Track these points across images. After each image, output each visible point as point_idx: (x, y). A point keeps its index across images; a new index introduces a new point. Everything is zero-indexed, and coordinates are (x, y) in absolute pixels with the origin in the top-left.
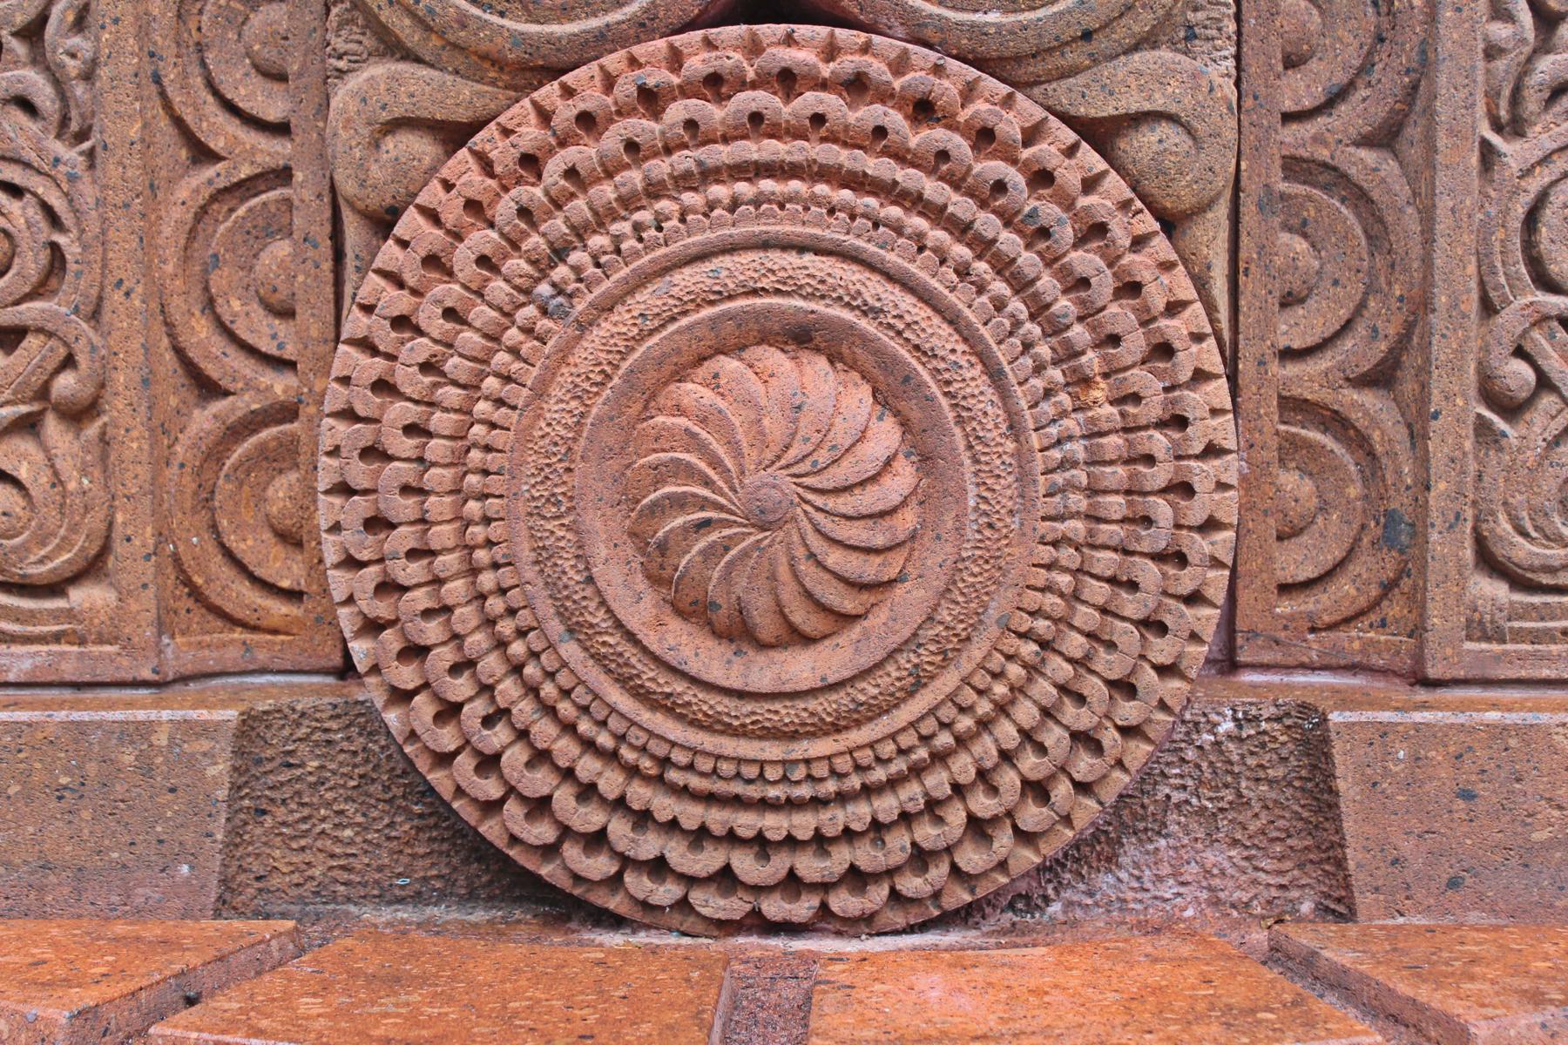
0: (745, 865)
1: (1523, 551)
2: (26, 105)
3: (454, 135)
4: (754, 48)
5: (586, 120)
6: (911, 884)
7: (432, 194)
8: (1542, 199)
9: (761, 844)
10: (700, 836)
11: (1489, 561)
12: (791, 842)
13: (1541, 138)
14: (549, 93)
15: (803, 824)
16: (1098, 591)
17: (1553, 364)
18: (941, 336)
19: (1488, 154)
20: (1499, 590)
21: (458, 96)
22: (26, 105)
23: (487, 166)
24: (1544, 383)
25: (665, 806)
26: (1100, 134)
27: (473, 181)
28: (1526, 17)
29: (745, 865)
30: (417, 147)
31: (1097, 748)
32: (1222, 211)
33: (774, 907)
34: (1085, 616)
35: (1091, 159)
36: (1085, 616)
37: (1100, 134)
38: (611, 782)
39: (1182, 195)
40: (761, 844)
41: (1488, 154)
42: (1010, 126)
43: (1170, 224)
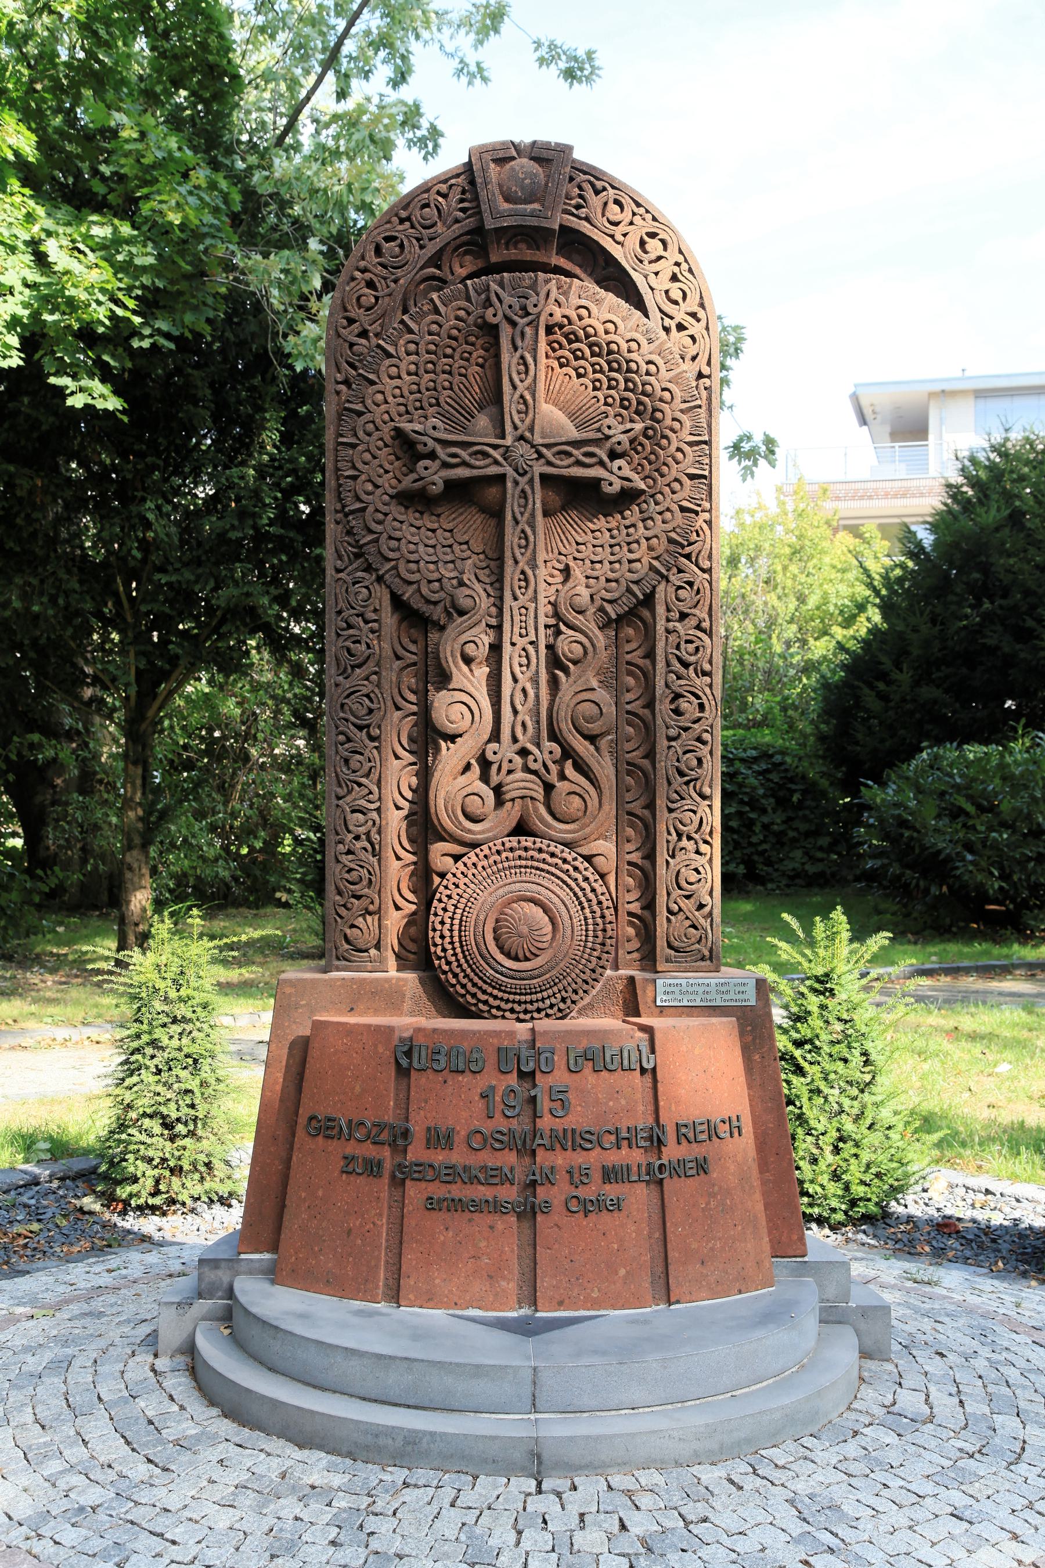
0: (517, 1007)
1: (676, 944)
2: (365, 849)
3: (457, 858)
4: (519, 842)
5: (486, 856)
6: (550, 1011)
7: (454, 870)
8: (678, 872)
9: (520, 1003)
10: (507, 1001)
11: (670, 946)
12: (526, 1002)
13: (678, 859)
14: (478, 850)
15: (528, 998)
16: (588, 951)
17: (682, 905)
18: (556, 900)
19: (667, 862)
20: (673, 952)
21: (457, 849)
22: (365, 849)
23: (465, 865)
24: (680, 910)
25: (500, 994)
26: (588, 859)
27: (462, 868)
28: (674, 834)
29: (517, 1007)
30: (450, 860)
31: (587, 983)
32: (613, 874)
33: (522, 1016)
34: (586, 956)
35: (587, 865)
36: (586, 956)
37: (588, 859)
38: (490, 990)
39: (605, 870)
40: (520, 1003)
41: (667, 862)
42: (569, 858)
43: (602, 876)
